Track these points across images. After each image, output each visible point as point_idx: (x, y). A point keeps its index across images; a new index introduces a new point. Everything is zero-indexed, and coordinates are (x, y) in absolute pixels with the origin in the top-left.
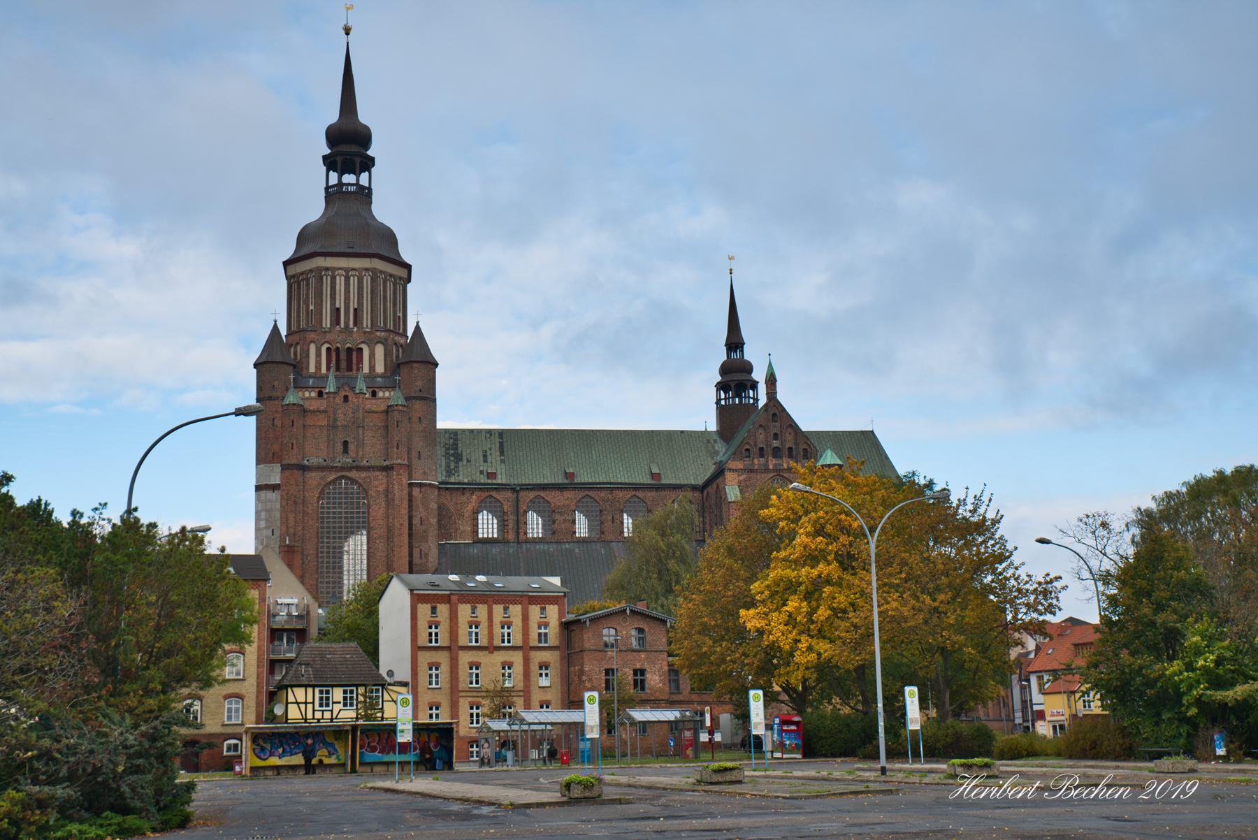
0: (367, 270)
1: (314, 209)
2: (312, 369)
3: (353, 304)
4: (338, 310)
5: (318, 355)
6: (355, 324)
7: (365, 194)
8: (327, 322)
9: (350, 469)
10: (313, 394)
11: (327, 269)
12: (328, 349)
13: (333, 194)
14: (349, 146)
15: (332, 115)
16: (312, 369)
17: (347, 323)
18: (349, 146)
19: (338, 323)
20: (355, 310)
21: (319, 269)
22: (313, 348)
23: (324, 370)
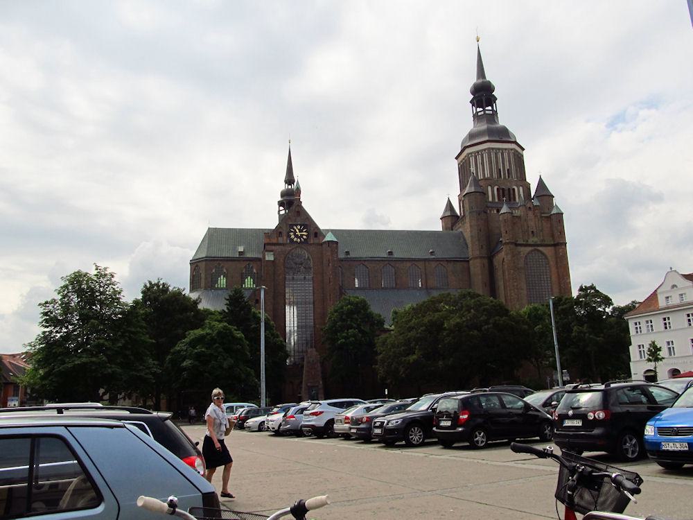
0: (512, 149)
2: (490, 199)
3: (507, 167)
4: (500, 170)
5: (493, 191)
6: (509, 177)
8: (495, 175)
9: (538, 245)
10: (495, 212)
12: (498, 189)
14: (483, 95)
15: (473, 79)
16: (490, 199)
17: (505, 177)
18: (483, 95)
19: (501, 177)
20: (508, 170)
21: (489, 149)
22: (489, 188)
23: (497, 200)
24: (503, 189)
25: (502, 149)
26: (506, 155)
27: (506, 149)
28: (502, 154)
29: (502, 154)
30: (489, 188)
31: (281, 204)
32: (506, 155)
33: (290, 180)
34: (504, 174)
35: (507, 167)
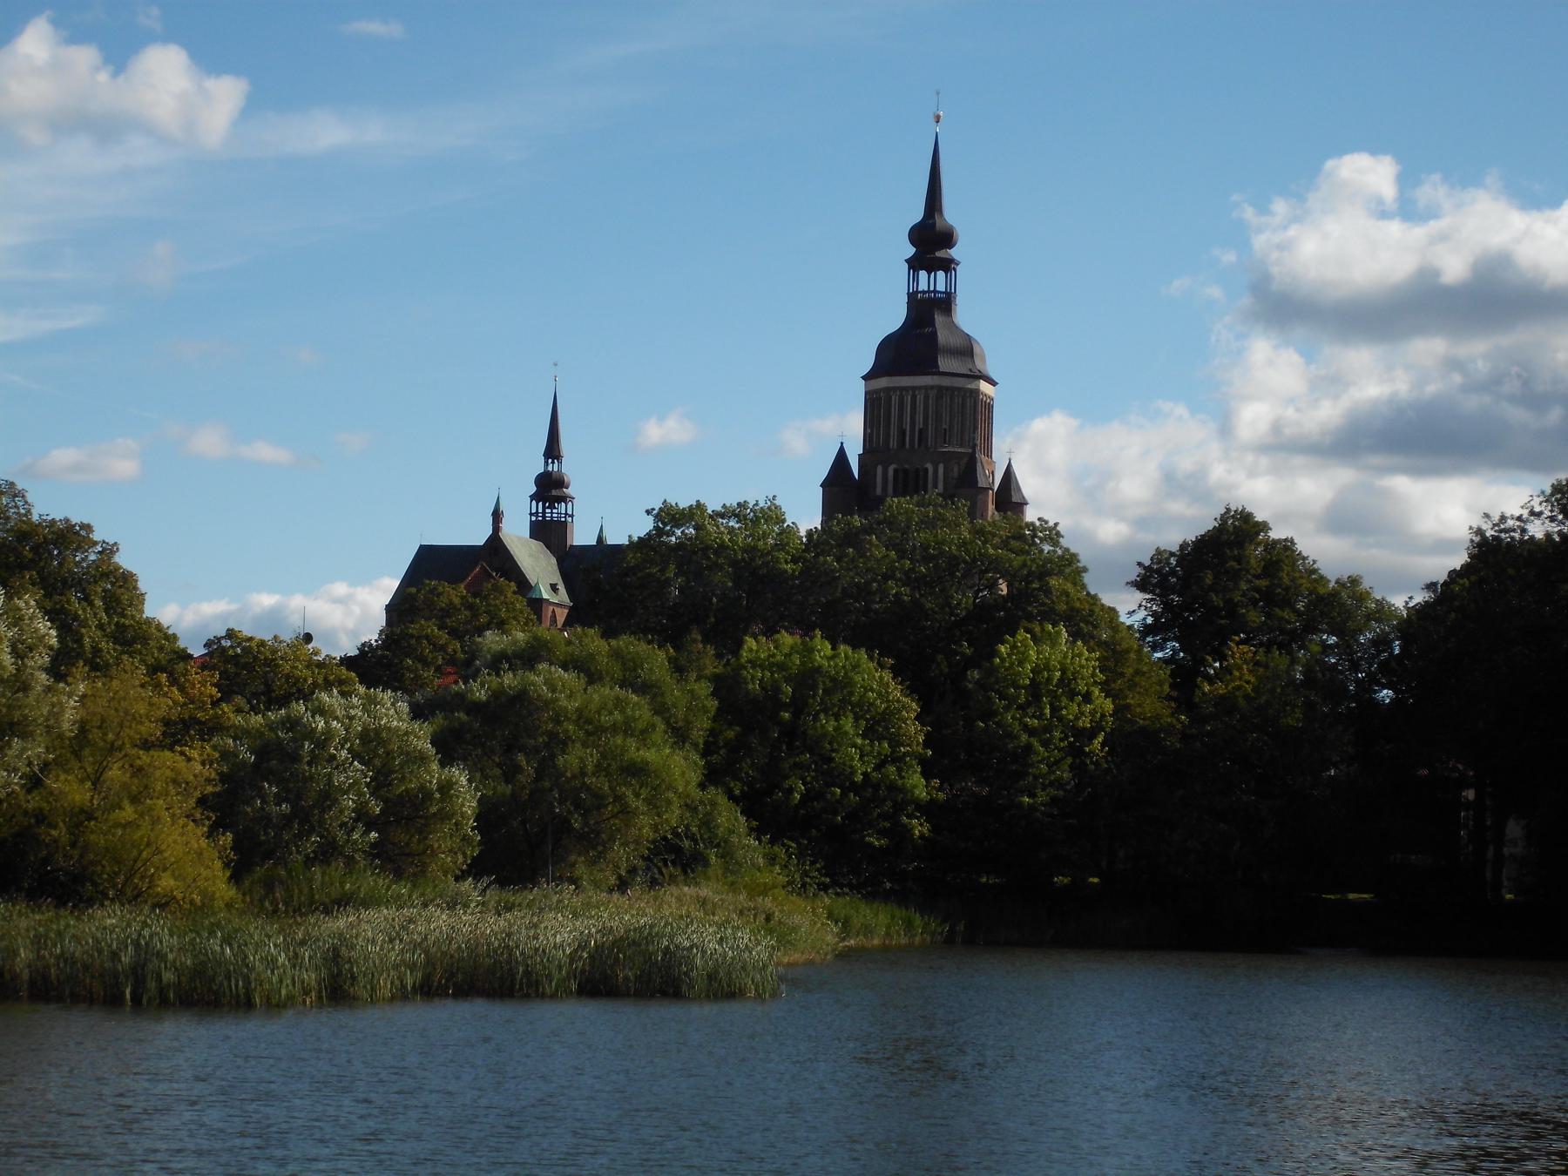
1: (894, 316)
2: (879, 491)
3: (919, 424)
4: (902, 433)
7: (945, 303)
8: (893, 444)
11: (894, 389)
12: (896, 471)
13: (914, 300)
16: (879, 491)
22: (879, 470)
24: (906, 472)
25: (914, 388)
26: (920, 398)
27: (920, 388)
28: (914, 398)
29: (914, 398)
30: (879, 470)
31: (532, 497)
32: (920, 398)
33: (553, 450)
34: (912, 439)
35: (919, 424)
